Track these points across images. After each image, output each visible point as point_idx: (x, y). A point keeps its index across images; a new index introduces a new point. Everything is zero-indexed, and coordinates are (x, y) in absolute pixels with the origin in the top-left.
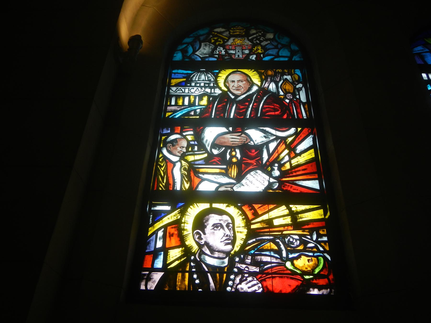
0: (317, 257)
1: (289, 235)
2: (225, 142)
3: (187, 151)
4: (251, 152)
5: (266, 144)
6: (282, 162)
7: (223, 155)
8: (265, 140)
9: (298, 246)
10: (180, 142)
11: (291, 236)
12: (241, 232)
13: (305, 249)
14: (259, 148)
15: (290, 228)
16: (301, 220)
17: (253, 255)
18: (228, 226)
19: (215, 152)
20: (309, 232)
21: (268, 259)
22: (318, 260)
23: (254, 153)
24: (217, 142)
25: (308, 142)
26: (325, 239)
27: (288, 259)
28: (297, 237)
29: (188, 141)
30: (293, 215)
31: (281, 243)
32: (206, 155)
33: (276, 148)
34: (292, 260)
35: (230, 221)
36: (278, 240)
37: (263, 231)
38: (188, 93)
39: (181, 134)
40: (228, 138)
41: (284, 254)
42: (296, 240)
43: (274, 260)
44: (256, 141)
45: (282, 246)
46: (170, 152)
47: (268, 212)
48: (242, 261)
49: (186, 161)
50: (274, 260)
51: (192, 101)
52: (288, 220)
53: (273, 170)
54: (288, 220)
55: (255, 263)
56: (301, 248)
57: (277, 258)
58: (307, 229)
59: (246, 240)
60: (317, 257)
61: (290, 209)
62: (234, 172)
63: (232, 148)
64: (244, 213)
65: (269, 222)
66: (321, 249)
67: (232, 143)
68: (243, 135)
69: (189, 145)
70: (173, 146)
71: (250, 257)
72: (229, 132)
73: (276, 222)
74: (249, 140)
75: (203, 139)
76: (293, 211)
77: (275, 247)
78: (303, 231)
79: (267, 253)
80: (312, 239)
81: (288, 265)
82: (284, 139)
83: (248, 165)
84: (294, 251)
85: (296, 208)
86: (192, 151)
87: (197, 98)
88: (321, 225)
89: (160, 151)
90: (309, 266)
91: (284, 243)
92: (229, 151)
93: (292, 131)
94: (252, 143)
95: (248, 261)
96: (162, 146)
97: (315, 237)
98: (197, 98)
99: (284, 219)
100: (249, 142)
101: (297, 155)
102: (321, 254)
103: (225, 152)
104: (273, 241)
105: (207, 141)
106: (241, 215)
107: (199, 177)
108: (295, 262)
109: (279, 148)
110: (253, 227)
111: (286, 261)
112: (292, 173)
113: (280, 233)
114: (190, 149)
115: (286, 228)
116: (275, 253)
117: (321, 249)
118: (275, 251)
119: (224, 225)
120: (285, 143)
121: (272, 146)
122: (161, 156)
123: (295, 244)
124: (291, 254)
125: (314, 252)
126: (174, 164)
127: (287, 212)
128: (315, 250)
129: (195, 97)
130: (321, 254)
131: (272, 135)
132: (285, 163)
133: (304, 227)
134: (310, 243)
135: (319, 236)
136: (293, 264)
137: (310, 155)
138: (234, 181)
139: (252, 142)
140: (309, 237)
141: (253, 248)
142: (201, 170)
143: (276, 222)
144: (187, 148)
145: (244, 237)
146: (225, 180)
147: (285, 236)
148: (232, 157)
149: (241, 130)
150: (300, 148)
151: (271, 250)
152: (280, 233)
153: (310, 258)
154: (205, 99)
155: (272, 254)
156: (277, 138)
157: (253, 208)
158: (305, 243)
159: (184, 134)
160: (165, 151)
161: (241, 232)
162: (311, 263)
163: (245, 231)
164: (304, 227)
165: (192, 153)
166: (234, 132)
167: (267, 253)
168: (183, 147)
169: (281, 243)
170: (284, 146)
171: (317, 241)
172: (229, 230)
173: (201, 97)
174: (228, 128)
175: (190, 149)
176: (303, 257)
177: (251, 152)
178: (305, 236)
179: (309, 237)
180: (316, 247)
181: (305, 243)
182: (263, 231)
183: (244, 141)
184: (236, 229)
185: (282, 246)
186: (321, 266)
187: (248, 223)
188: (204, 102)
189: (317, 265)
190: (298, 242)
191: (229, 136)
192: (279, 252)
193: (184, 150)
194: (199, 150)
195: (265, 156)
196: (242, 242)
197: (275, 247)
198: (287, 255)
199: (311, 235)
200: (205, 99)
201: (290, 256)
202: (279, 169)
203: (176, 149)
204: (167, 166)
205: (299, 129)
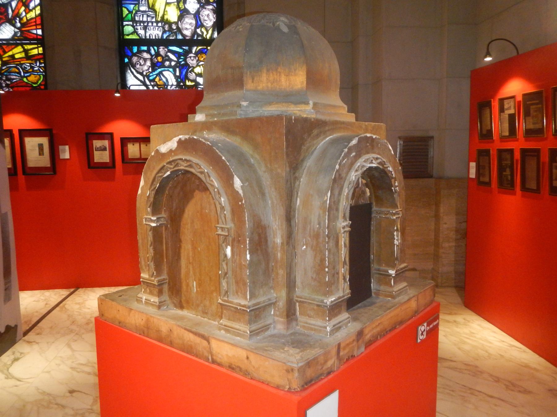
0: (39, 75)
1: (24, 63)
9: (29, 69)
11: (26, 64)
13: (33, 71)
16: (30, 54)
17: (6, 76)
21: (14, 77)
22: (40, 77)
26: (43, 65)
27: (24, 77)
30: (26, 51)
31: (20, 68)
33: (17, 5)
34: (26, 77)
36: (18, 67)
37: (10, 61)
41: (22, 74)
42: (28, 66)
45: (21, 70)
47: (11, 50)
50: (17, 78)
52: (23, 55)
54: (23, 55)
56: (31, 70)
57: (18, 76)
60: (39, 75)
61: (23, 48)
65: (13, 56)
66: (42, 71)
71: (5, 76)
73: (17, 56)
76: (26, 49)
77: (17, 71)
78: (32, 61)
79: (14, 74)
80: (36, 65)
81: (25, 80)
84: (27, 72)
85: (26, 47)
88: (41, 57)
90: (35, 80)
95: (4, 78)
97: (38, 64)
99: (21, 54)
101: (31, 10)
102: (42, 73)
104: (16, 67)
108: (28, 78)
111: (23, 78)
113: (19, 63)
115: (22, 59)
116: (18, 74)
117: (42, 71)
118: (17, 73)
123: (28, 68)
124: (26, 74)
125: (38, 72)
127: (22, 50)
128: (38, 71)
130: (42, 73)
132: (23, 17)
133: (32, 59)
134: (35, 67)
135: (40, 63)
136: (27, 79)
137: (38, 11)
140: (35, 64)
141: (5, 72)
143: (17, 56)
152: (19, 63)
153: (36, 76)
158: (32, 68)
162: (37, 78)
167: (14, 74)
169: (20, 68)
170: (21, 4)
171: (39, 67)
176: (32, 75)
178: (32, 64)
179: (35, 64)
180: (39, 70)
181: (32, 68)
182: (10, 61)
185: (21, 70)
186: (42, 79)
189: (39, 79)
190: (29, 67)
192: (19, 73)
195: (10, 11)
197: (17, 71)
198: (24, 74)
201: (26, 75)
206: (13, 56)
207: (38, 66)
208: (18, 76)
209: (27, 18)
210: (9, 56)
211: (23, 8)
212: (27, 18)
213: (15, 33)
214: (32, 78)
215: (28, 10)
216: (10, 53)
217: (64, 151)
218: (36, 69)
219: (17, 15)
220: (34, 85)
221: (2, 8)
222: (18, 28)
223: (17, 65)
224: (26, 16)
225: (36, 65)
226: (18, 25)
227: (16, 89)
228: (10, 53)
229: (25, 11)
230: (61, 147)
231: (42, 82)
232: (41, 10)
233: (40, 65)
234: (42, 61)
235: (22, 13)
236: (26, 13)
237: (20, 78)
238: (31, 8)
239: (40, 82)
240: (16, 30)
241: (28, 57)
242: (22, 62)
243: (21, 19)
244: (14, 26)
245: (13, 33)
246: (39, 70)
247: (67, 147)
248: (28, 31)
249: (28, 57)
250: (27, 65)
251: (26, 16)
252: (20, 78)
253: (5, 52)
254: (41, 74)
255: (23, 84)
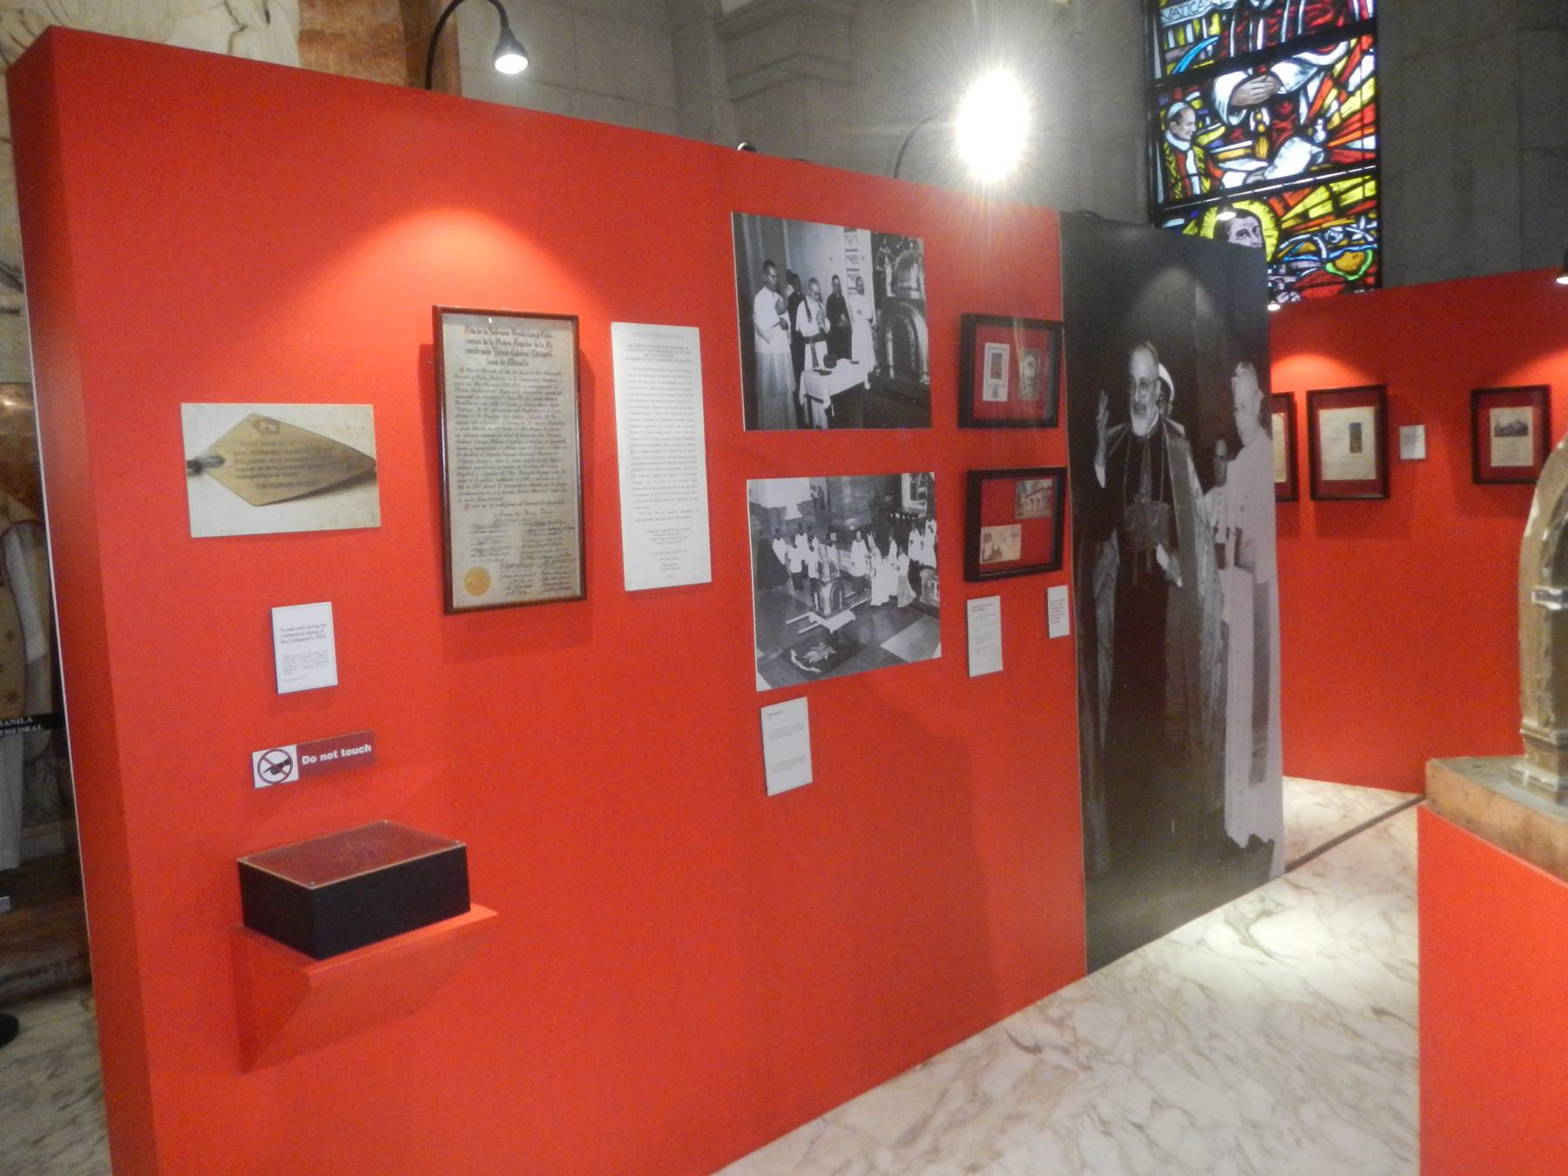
1: (1329, 228)
2: (1244, 100)
3: (1198, 129)
4: (1282, 107)
5: (1304, 87)
6: (1328, 115)
7: (1245, 122)
8: (1302, 79)
9: (1341, 241)
10: (1184, 116)
12: (1270, 236)
13: (1349, 245)
14: (1293, 97)
15: (1332, 218)
16: (1345, 203)
18: (1254, 230)
19: (1235, 121)
20: (1355, 219)
22: (1366, 256)
23: (1288, 107)
24: (1235, 102)
25: (1368, 63)
26: (1374, 224)
27: (1329, 260)
28: (1340, 229)
29: (1196, 111)
30: (1335, 198)
31: (1320, 241)
32: (1222, 130)
33: (1319, 90)
34: (1333, 261)
35: (1256, 224)
38: (1189, 15)
39: (1183, 100)
40: (1248, 90)
42: (1339, 232)
43: (1313, 265)
44: (1288, 84)
45: (1322, 245)
46: (1177, 137)
48: (1275, 273)
49: (1199, 145)
50: (1313, 265)
51: (1197, 32)
53: (1315, 131)
54: (1328, 207)
55: (1291, 272)
57: (1315, 261)
58: (1352, 214)
59: (1277, 246)
60: (1364, 251)
61: (1329, 189)
62: (1263, 149)
63: (1254, 108)
64: (1272, 210)
65: (1304, 216)
67: (1256, 97)
68: (1270, 78)
69: (1200, 118)
70: (1178, 124)
71: (1284, 266)
72: (1250, 78)
73: (1313, 214)
74: (1278, 86)
75: (1214, 100)
77: (1312, 248)
78: (1348, 219)
80: (1358, 228)
81: (1330, 267)
82: (1329, 69)
83: (1283, 130)
84: (1336, 248)
85: (1336, 187)
86: (1205, 127)
87: (1204, 21)
89: (1162, 139)
91: (1323, 239)
92: (1252, 114)
93: (1342, 48)
94: (1283, 91)
95: (1283, 271)
96: (1163, 128)
98: (1204, 21)
100: (1279, 90)
101: (1352, 94)
103: (1248, 116)
104: (1310, 240)
105: (1220, 103)
106: (1268, 212)
107: (1219, 168)
108: (1338, 262)
109: (1323, 87)
110: (1285, 226)
112: (1342, 130)
113: (1317, 228)
114: (1200, 125)
119: (1250, 230)
120: (1332, 75)
121: (1312, 88)
122: (1166, 145)
126: (1185, 153)
128: (1362, 242)
129: (1200, 19)
130: (1369, 246)
131: (1312, 65)
135: (1369, 221)
136: (1335, 265)
137: (1368, 91)
138: (1264, 164)
139: (1282, 89)
140: (1354, 226)
141: (1286, 255)
142: (1221, 156)
143: (1313, 214)
144: (1197, 123)
145: (1275, 242)
146: (1253, 165)
147: (1324, 231)
148: (1259, 122)
149: (1264, 70)
150: (1354, 80)
151: (1309, 252)
152: (1317, 228)
154: (1216, 19)
155: (1311, 257)
156: (1321, 68)
157: (1282, 199)
158: (1348, 235)
159: (1188, 99)
160: (1170, 137)
161: (1270, 236)
162: (1357, 260)
163: (1276, 233)
164: (1349, 213)
165: (1203, 131)
166: (1256, 74)
168: (1191, 123)
169: (1320, 241)
170: (1330, 83)
172: (1257, 235)
173: (1209, 17)
174: (1246, 72)
175: (1200, 125)
176: (1348, 254)
177: (1282, 107)
181: (1348, 235)
183: (1272, 90)
184: (1265, 233)
185: (1322, 245)
187: (1278, 221)
188: (1215, 29)
189: (1364, 262)
190: (1341, 236)
191: (1248, 86)
192: (1318, 253)
193: (1193, 128)
194: (1212, 124)
195: (1303, 109)
196: (1273, 249)
197: (1312, 248)
198: (1328, 254)
199: (1358, 222)
200: (1216, 19)
201: (1332, 255)
202: (1325, 128)
203: (1182, 128)
204: (1177, 161)
205: (1353, 42)
206: (1304, 216)
207: (1361, 230)
208: (1315, 261)
209: (1341, 115)
210: (1297, 216)
211: (1334, 92)
212: (1341, 115)
213: (1314, 157)
214: (1347, 261)
215: (1345, 94)
216: (1299, 209)
217: (1412, 440)
218: (1355, 237)
219: (1319, 113)
220: (1351, 278)
221: (1286, 104)
222: (1320, 145)
223: (1314, 233)
224: (1339, 110)
225: (1358, 228)
226: (1321, 136)
227: (1308, 292)
228: (1299, 209)
229: (1337, 98)
230: (1405, 431)
231: (1370, 266)
232: (1377, 87)
233: (1368, 227)
234: (1372, 216)
235: (1329, 107)
236: (1341, 104)
237: (1318, 264)
238: (1351, 88)
239: (1364, 268)
240: (1316, 150)
241: (1340, 211)
242: (1324, 226)
243: (1328, 121)
244: (1310, 139)
245: (1307, 158)
246: (1364, 238)
247: (1420, 431)
248: (1344, 146)
249: (1340, 210)
250: (1337, 233)
251: (1339, 110)
252: (1318, 264)
253: (1288, 208)
254: (1369, 248)
255: (1325, 279)
